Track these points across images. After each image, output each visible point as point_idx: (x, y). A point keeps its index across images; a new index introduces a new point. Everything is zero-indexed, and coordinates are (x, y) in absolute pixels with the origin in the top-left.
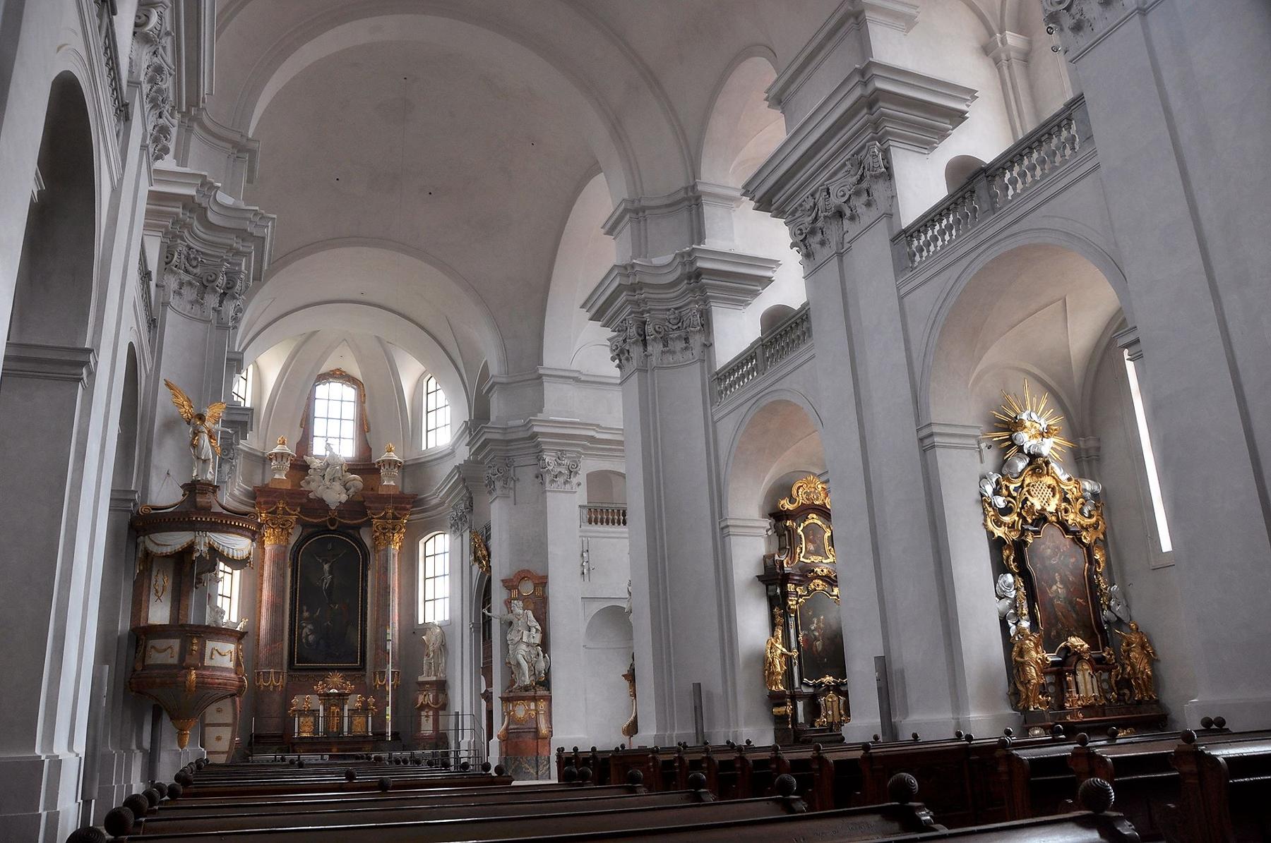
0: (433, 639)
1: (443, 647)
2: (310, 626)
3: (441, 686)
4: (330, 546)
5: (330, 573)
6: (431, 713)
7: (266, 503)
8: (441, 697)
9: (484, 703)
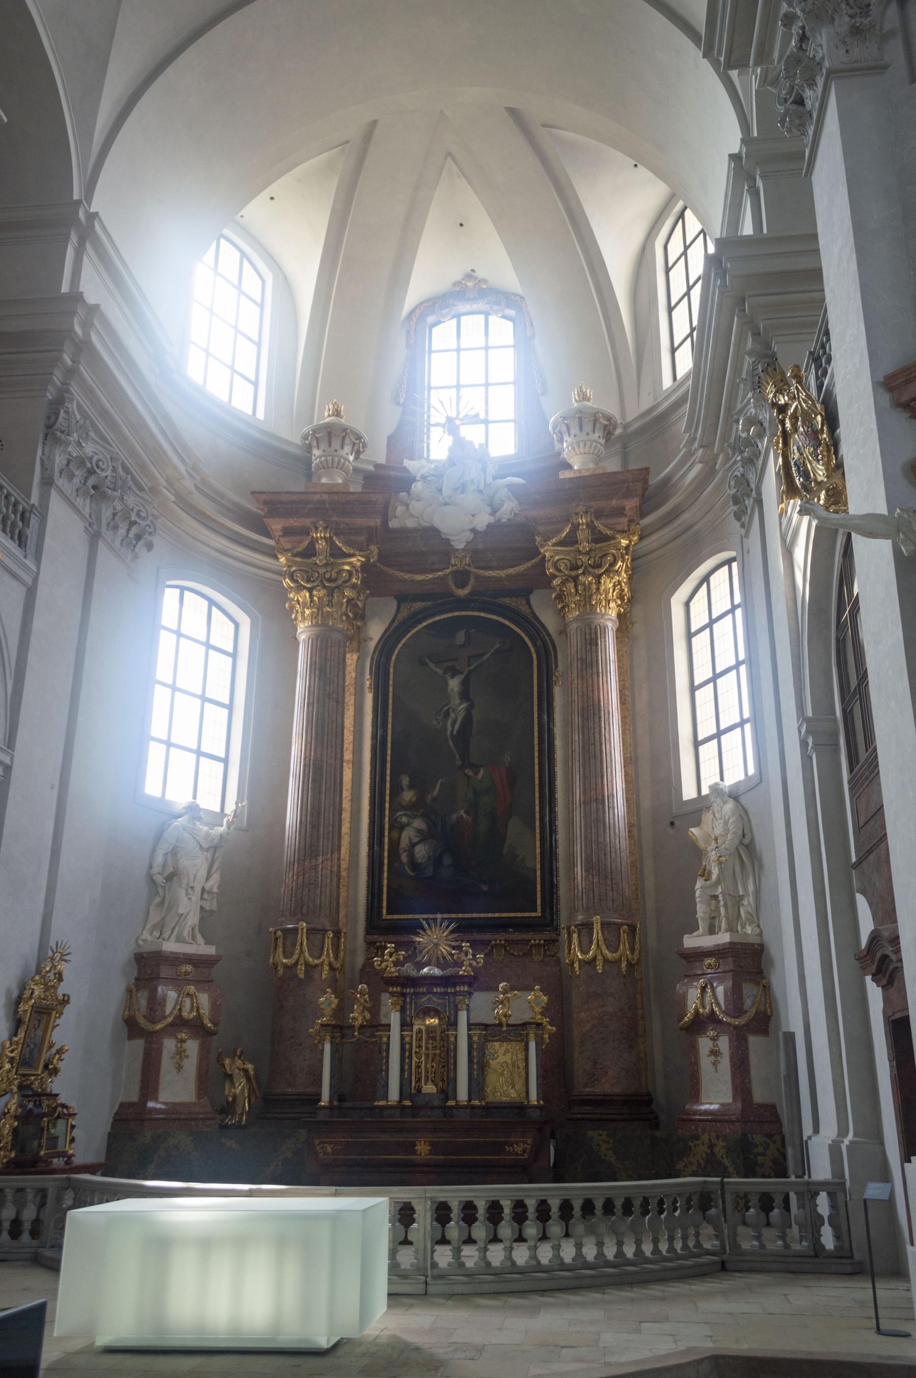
0: (718, 830)
1: (747, 851)
2: (419, 824)
3: (749, 962)
4: (460, 637)
5: (465, 695)
6: (724, 1043)
7: (288, 532)
8: (750, 991)
9: (875, 994)
